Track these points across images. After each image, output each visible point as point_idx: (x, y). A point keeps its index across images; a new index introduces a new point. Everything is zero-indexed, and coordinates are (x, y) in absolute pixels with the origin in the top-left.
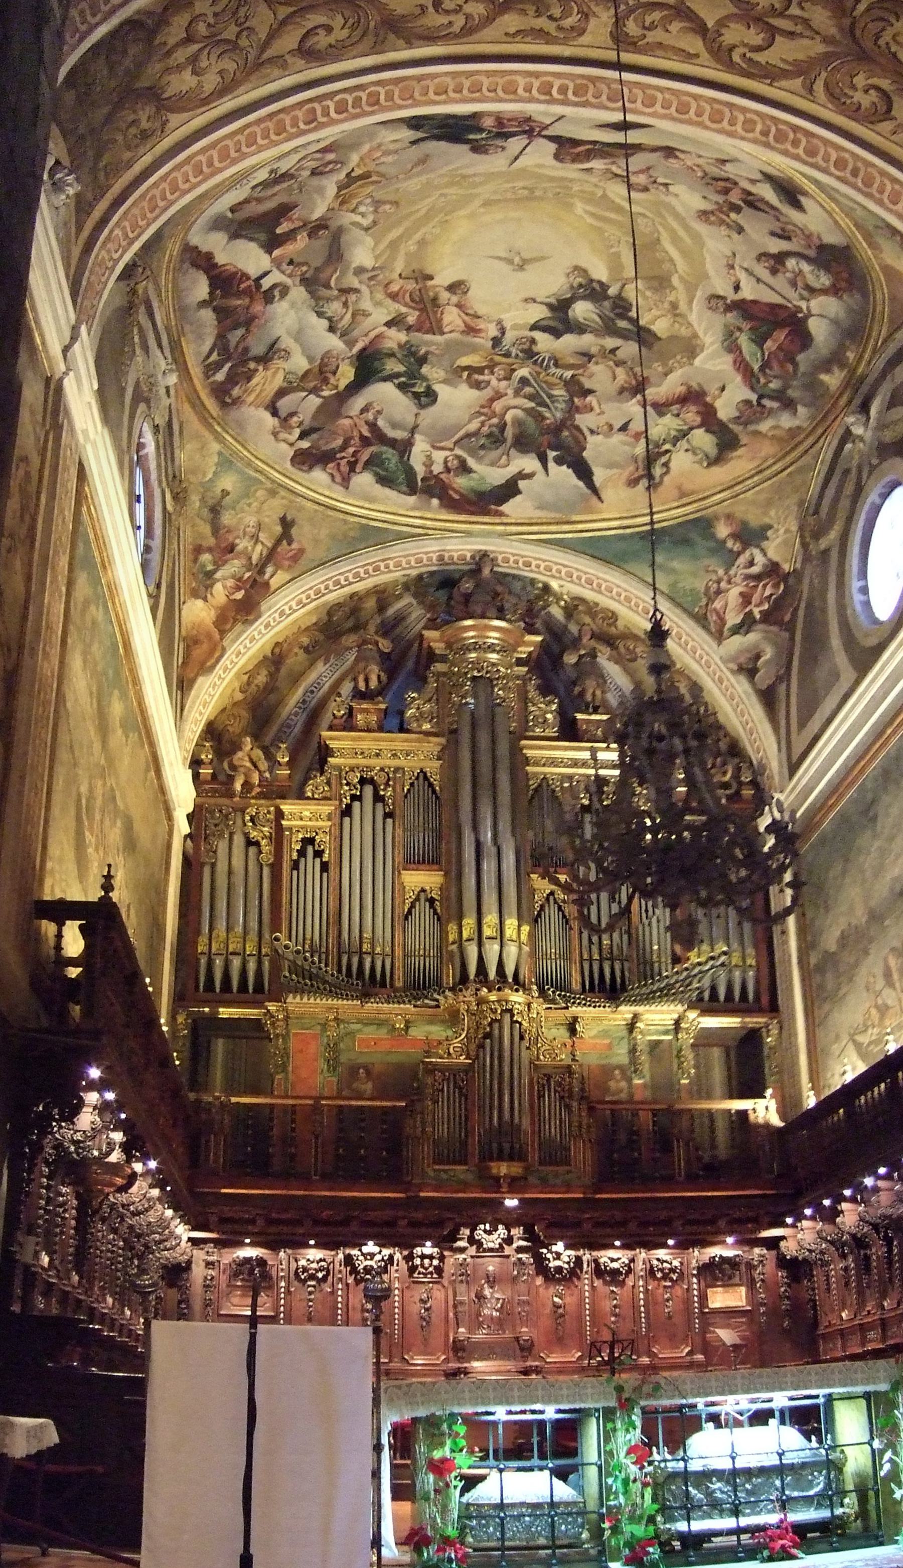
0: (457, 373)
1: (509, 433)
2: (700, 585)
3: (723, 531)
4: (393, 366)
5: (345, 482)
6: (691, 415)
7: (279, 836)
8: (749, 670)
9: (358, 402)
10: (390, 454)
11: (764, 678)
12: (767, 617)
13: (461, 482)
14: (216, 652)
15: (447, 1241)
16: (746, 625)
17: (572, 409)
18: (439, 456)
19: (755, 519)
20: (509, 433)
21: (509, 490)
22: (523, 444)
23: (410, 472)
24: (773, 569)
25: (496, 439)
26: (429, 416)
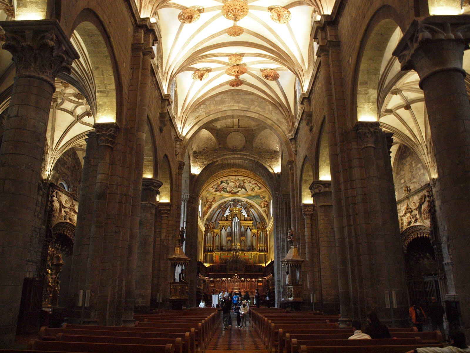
0: (231, 182)
1: (237, 187)
2: (259, 202)
3: (261, 196)
4: (224, 182)
5: (220, 192)
6: (256, 185)
7: (214, 233)
8: (265, 212)
9: (221, 185)
10: (225, 189)
11: (267, 213)
12: (266, 206)
13: (233, 191)
14: (207, 213)
15: (231, 278)
16: (264, 207)
17: (244, 184)
18: (230, 189)
19: (264, 196)
20: (237, 187)
21: (238, 192)
22: (239, 187)
23: (227, 191)
24: (266, 201)
25: (236, 187)
26: (229, 185)
